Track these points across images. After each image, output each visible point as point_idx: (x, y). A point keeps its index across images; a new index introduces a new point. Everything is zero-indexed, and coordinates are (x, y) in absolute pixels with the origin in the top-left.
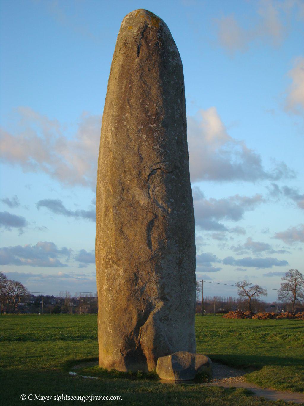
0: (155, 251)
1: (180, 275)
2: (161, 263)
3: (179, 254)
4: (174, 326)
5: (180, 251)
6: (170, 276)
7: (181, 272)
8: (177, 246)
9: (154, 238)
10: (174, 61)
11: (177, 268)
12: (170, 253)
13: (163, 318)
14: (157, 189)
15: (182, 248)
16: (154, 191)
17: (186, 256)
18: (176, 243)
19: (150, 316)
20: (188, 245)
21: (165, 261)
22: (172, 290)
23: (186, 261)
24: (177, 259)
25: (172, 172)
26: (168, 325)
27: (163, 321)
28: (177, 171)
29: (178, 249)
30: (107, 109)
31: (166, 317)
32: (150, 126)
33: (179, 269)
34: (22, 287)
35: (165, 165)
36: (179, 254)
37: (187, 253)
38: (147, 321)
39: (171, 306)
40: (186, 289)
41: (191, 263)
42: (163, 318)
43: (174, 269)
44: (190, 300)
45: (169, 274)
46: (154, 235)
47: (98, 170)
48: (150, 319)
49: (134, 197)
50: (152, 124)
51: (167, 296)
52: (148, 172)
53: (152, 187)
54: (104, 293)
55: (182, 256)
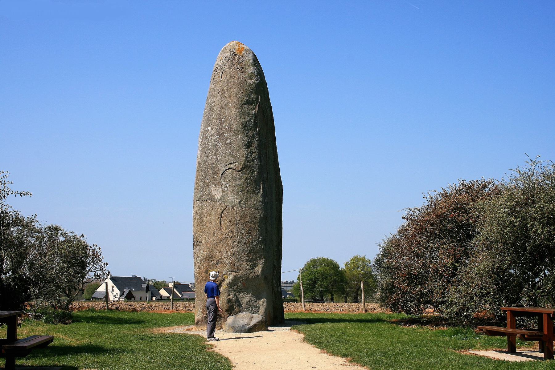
1: (249, 253)
14: (229, 184)
46: (225, 222)
49: (211, 192)
51: (237, 270)
52: (221, 172)
53: (224, 183)
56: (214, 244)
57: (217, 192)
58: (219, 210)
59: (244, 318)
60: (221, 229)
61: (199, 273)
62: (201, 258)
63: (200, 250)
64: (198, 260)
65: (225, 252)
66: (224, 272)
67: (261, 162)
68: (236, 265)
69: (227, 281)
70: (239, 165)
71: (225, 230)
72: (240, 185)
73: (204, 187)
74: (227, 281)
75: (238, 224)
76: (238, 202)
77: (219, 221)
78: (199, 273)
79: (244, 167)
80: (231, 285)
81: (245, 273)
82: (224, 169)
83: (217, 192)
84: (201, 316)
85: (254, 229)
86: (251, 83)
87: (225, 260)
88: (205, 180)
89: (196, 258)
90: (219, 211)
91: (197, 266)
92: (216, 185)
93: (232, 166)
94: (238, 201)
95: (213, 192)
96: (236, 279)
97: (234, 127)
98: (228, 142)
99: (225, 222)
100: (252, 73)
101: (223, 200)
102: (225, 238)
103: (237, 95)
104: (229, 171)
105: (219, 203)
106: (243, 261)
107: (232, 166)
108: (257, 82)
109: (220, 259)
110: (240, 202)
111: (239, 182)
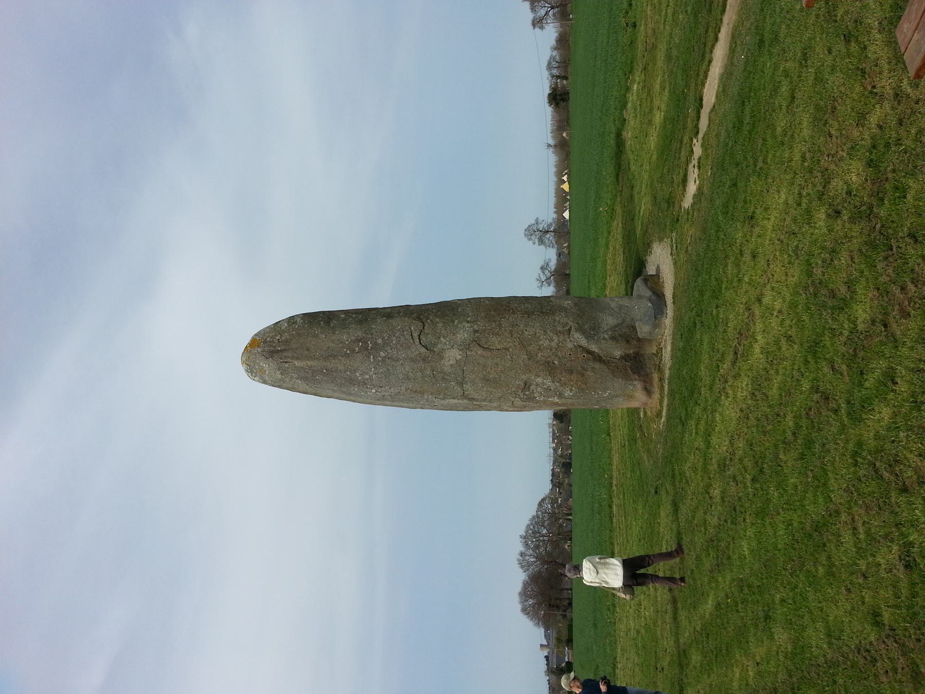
14: (442, 339)
30: (351, 398)
34: (543, 500)
38: (596, 350)
47: (422, 408)
48: (594, 348)
52: (423, 350)
54: (563, 401)
56: (529, 359)
57: (453, 355)
58: (479, 353)
60: (507, 349)
62: (548, 382)
65: (541, 342)
68: (559, 328)
69: (583, 342)
72: (444, 323)
74: (583, 342)
75: (500, 325)
76: (469, 325)
79: (419, 318)
80: (589, 337)
81: (571, 319)
83: (453, 355)
84: (636, 382)
88: (434, 376)
92: (442, 358)
93: (416, 335)
94: (467, 325)
95: (451, 362)
96: (580, 329)
98: (380, 341)
99: (495, 342)
101: (465, 347)
102: (521, 343)
103: (316, 336)
104: (423, 338)
105: (468, 353)
106: (555, 320)
110: (468, 322)
111: (440, 325)
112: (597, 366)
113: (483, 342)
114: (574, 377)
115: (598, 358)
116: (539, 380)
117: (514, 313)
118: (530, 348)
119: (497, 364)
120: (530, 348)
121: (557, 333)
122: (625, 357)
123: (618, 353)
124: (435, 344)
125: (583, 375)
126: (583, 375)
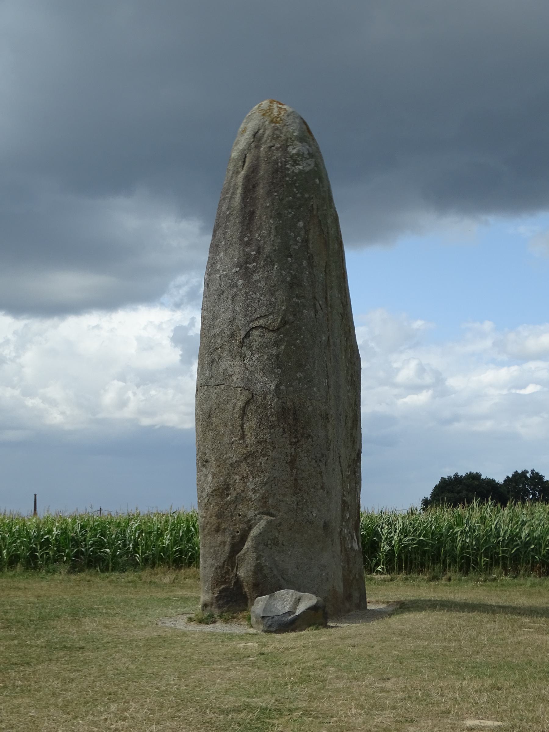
0: (252, 446)
1: (296, 480)
2: (261, 463)
3: (291, 448)
4: (289, 553)
5: (291, 444)
6: (276, 481)
7: (296, 474)
8: (286, 438)
9: (251, 427)
10: (297, 167)
11: (289, 469)
12: (274, 448)
13: (269, 542)
15: (294, 440)
16: (252, 360)
17: (302, 451)
18: (284, 432)
19: (249, 539)
20: (305, 435)
21: (267, 460)
22: (280, 501)
23: (303, 458)
24: (287, 456)
25: (278, 329)
26: (279, 552)
27: (270, 546)
28: (287, 326)
29: (288, 442)
31: (274, 540)
32: (249, 267)
33: (292, 471)
35: (268, 321)
36: (291, 448)
37: (304, 446)
38: (245, 547)
39: (280, 524)
40: (306, 500)
41: (314, 461)
42: (269, 542)
43: (283, 470)
44: (314, 515)
45: (274, 478)
48: (248, 544)
49: (225, 370)
50: (250, 264)
51: (272, 511)
52: (243, 333)
53: (248, 353)
55: (295, 452)
56: (231, 465)
59: (286, 601)
60: (243, 436)
61: (205, 517)
62: (208, 489)
63: (206, 476)
64: (204, 494)
65: (251, 479)
66: (250, 514)
67: (316, 312)
69: (254, 532)
70: (274, 321)
71: (250, 439)
72: (277, 356)
73: (213, 361)
75: (272, 427)
76: (273, 388)
77: (239, 423)
78: (205, 517)
79: (284, 323)
82: (248, 328)
85: (302, 436)
86: (296, 171)
87: (250, 493)
89: (201, 489)
90: (240, 404)
91: (203, 504)
93: (262, 322)
97: (268, 249)
99: (251, 422)
100: (298, 154)
104: (257, 332)
107: (262, 322)
108: (308, 169)
109: (243, 491)
110: (277, 387)
111: (274, 352)
112: (227, 548)
113: (253, 407)
114: (214, 520)
115: (236, 547)
116: (210, 478)
117: (291, 443)
118: (243, 465)
119: (226, 426)
120: (243, 465)
121: (264, 500)
122: (238, 583)
123: (242, 573)
124: (249, 347)
125: (217, 530)
126: (217, 530)
